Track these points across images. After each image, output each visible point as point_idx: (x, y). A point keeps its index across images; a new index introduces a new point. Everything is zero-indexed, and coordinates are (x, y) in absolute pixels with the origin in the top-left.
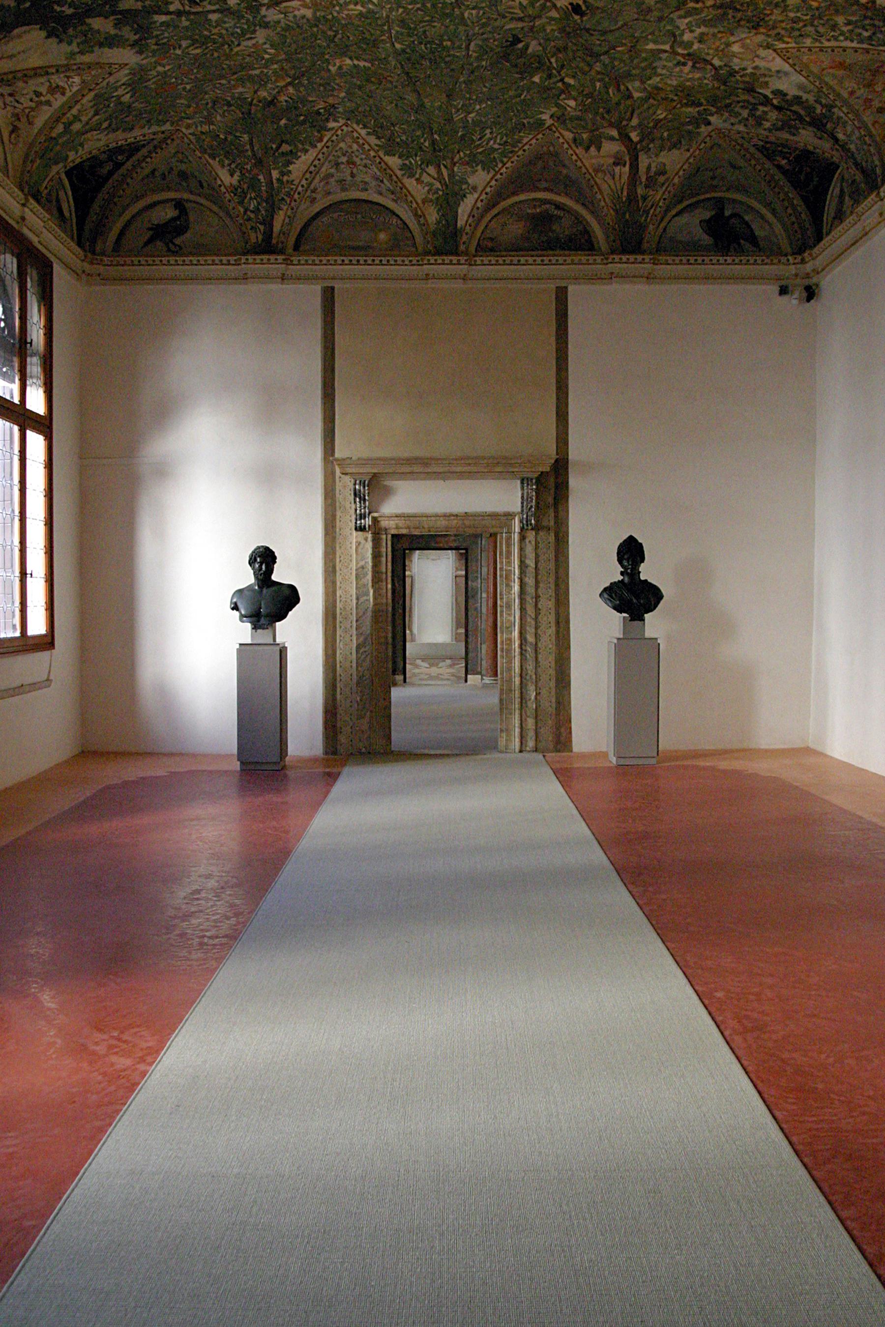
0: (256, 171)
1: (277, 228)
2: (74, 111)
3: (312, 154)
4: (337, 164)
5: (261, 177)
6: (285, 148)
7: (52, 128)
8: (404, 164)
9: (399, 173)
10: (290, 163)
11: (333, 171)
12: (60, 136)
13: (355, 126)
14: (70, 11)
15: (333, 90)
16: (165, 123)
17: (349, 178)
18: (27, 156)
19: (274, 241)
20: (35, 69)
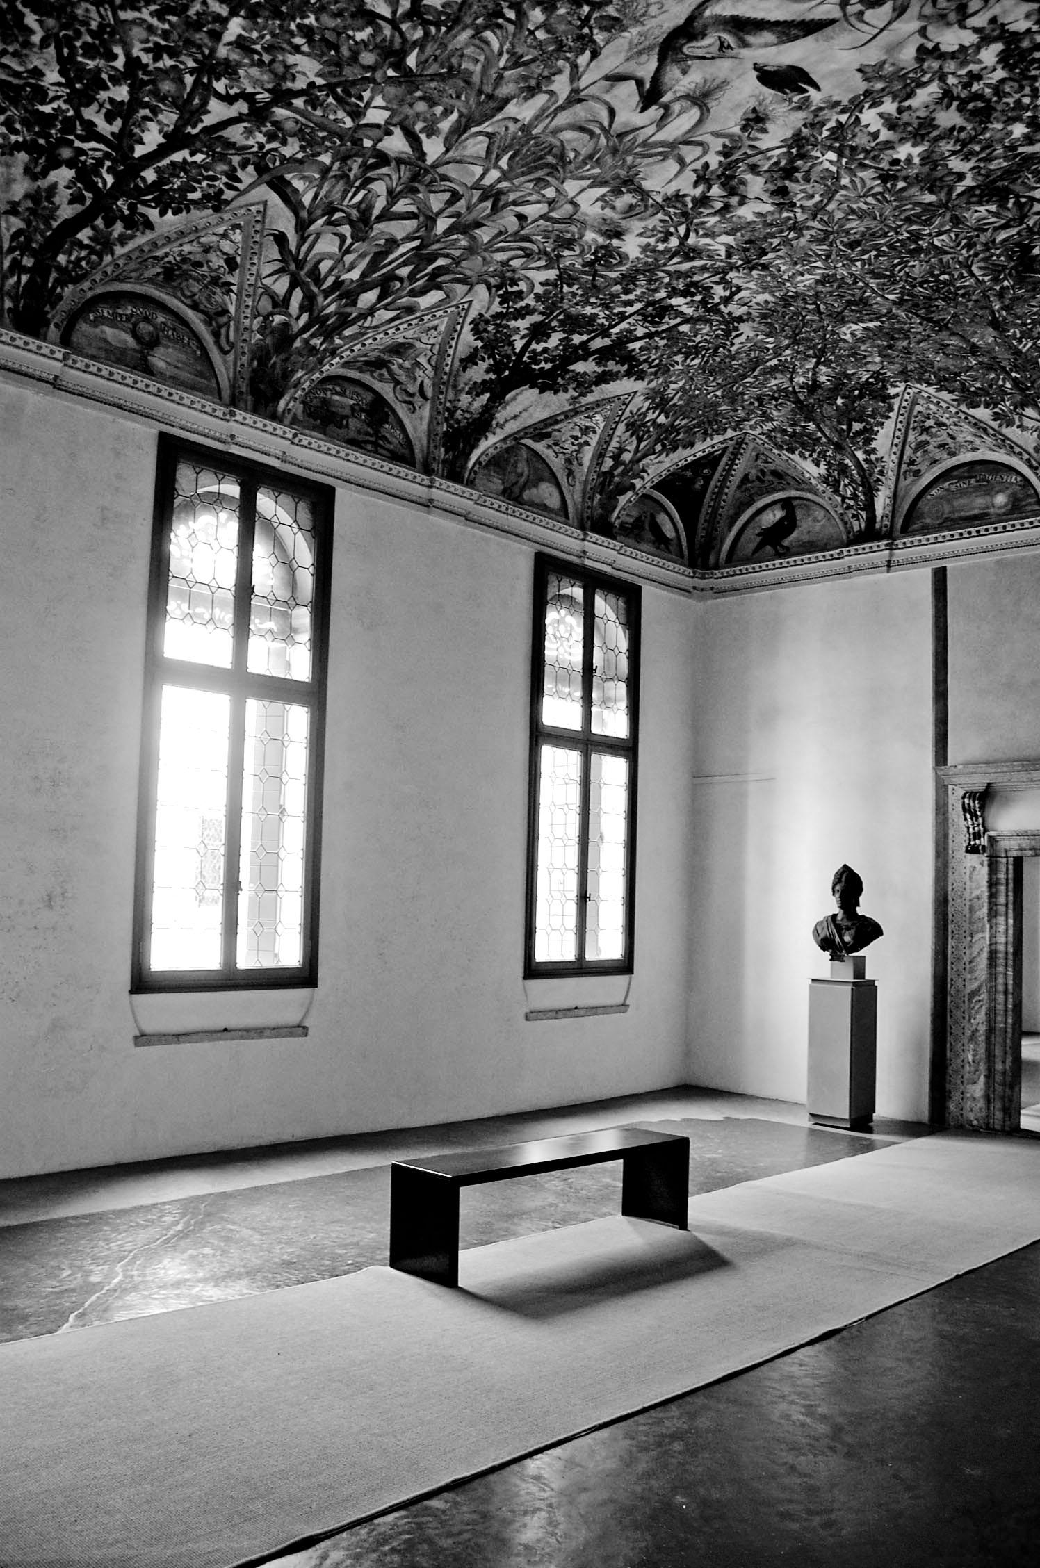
0: (839, 457)
1: (879, 512)
2: (614, 444)
3: (889, 425)
4: (926, 430)
5: (847, 461)
6: (857, 426)
7: (601, 464)
8: (996, 413)
9: (995, 424)
10: (868, 441)
11: (924, 437)
12: (614, 468)
13: (918, 385)
14: (549, 366)
15: (865, 357)
16: (725, 430)
17: (949, 441)
18: (584, 492)
19: (877, 526)
20: (543, 421)
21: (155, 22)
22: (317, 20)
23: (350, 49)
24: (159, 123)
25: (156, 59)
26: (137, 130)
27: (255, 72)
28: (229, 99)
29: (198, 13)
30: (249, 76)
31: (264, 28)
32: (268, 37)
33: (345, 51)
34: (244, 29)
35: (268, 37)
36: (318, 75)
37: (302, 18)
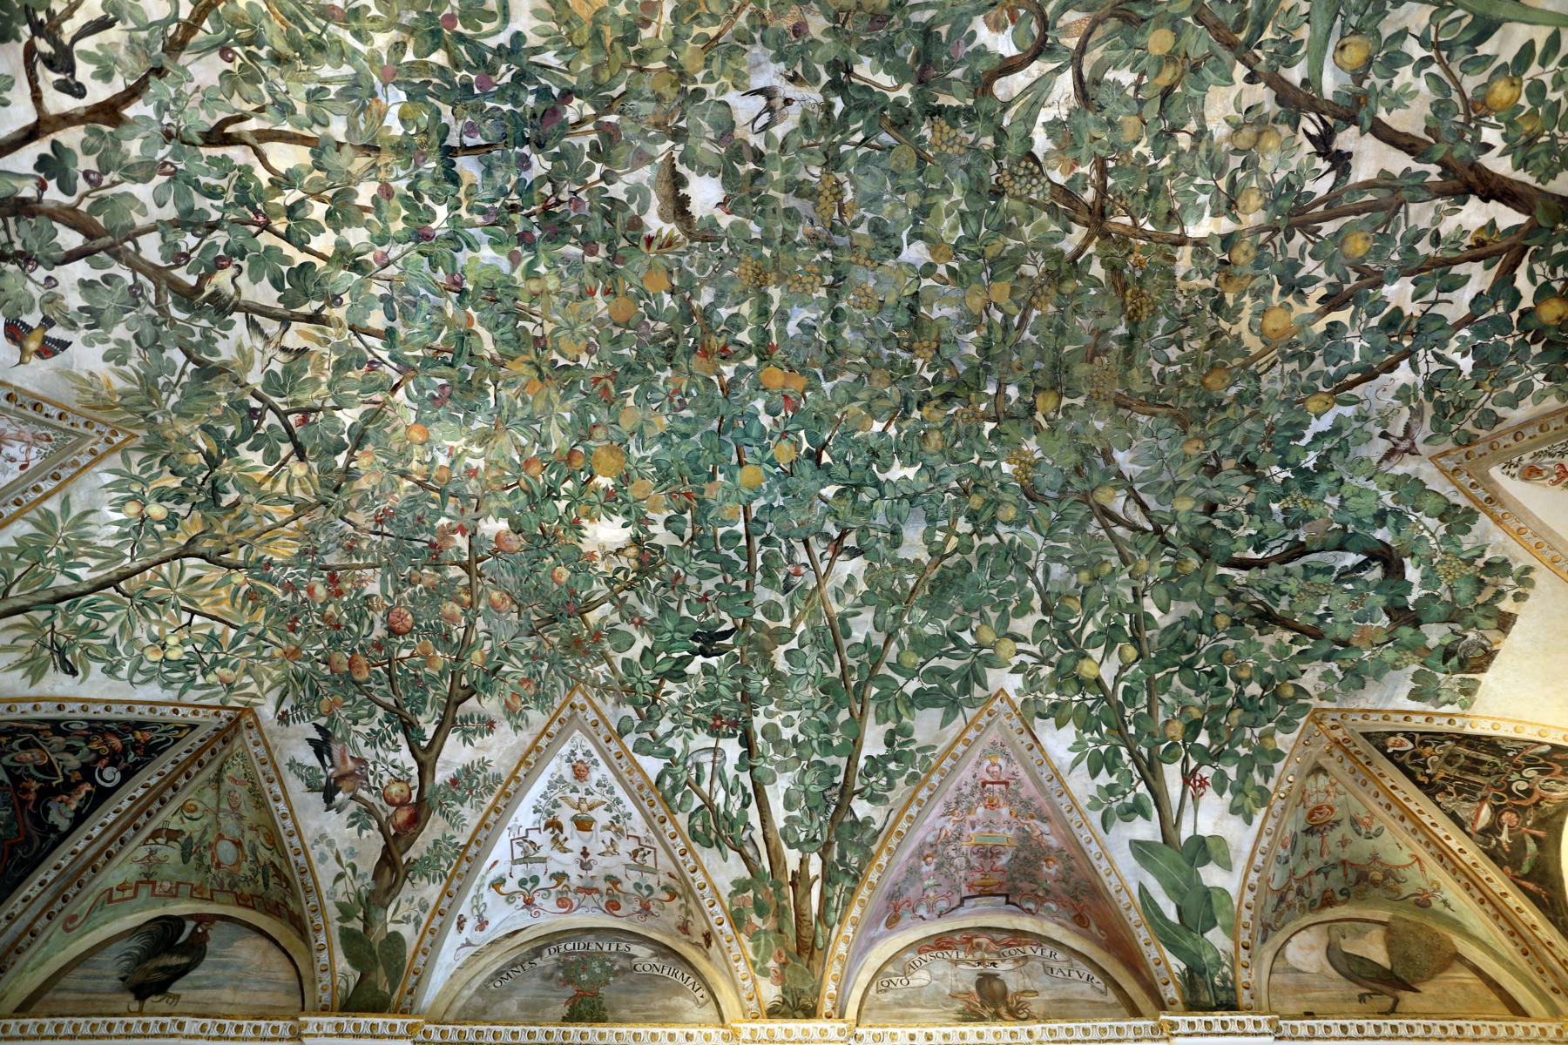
21: (1246, 315)
22: (1137, 142)
23: (1159, 72)
24: (1438, 220)
25: (1315, 280)
26: (1468, 241)
27: (1267, 164)
28: (1341, 162)
29: (1206, 276)
30: (1282, 162)
31: (1186, 193)
32: (1198, 181)
33: (1168, 75)
34: (1201, 216)
35: (1198, 181)
36: (1231, 80)
37: (1145, 160)
